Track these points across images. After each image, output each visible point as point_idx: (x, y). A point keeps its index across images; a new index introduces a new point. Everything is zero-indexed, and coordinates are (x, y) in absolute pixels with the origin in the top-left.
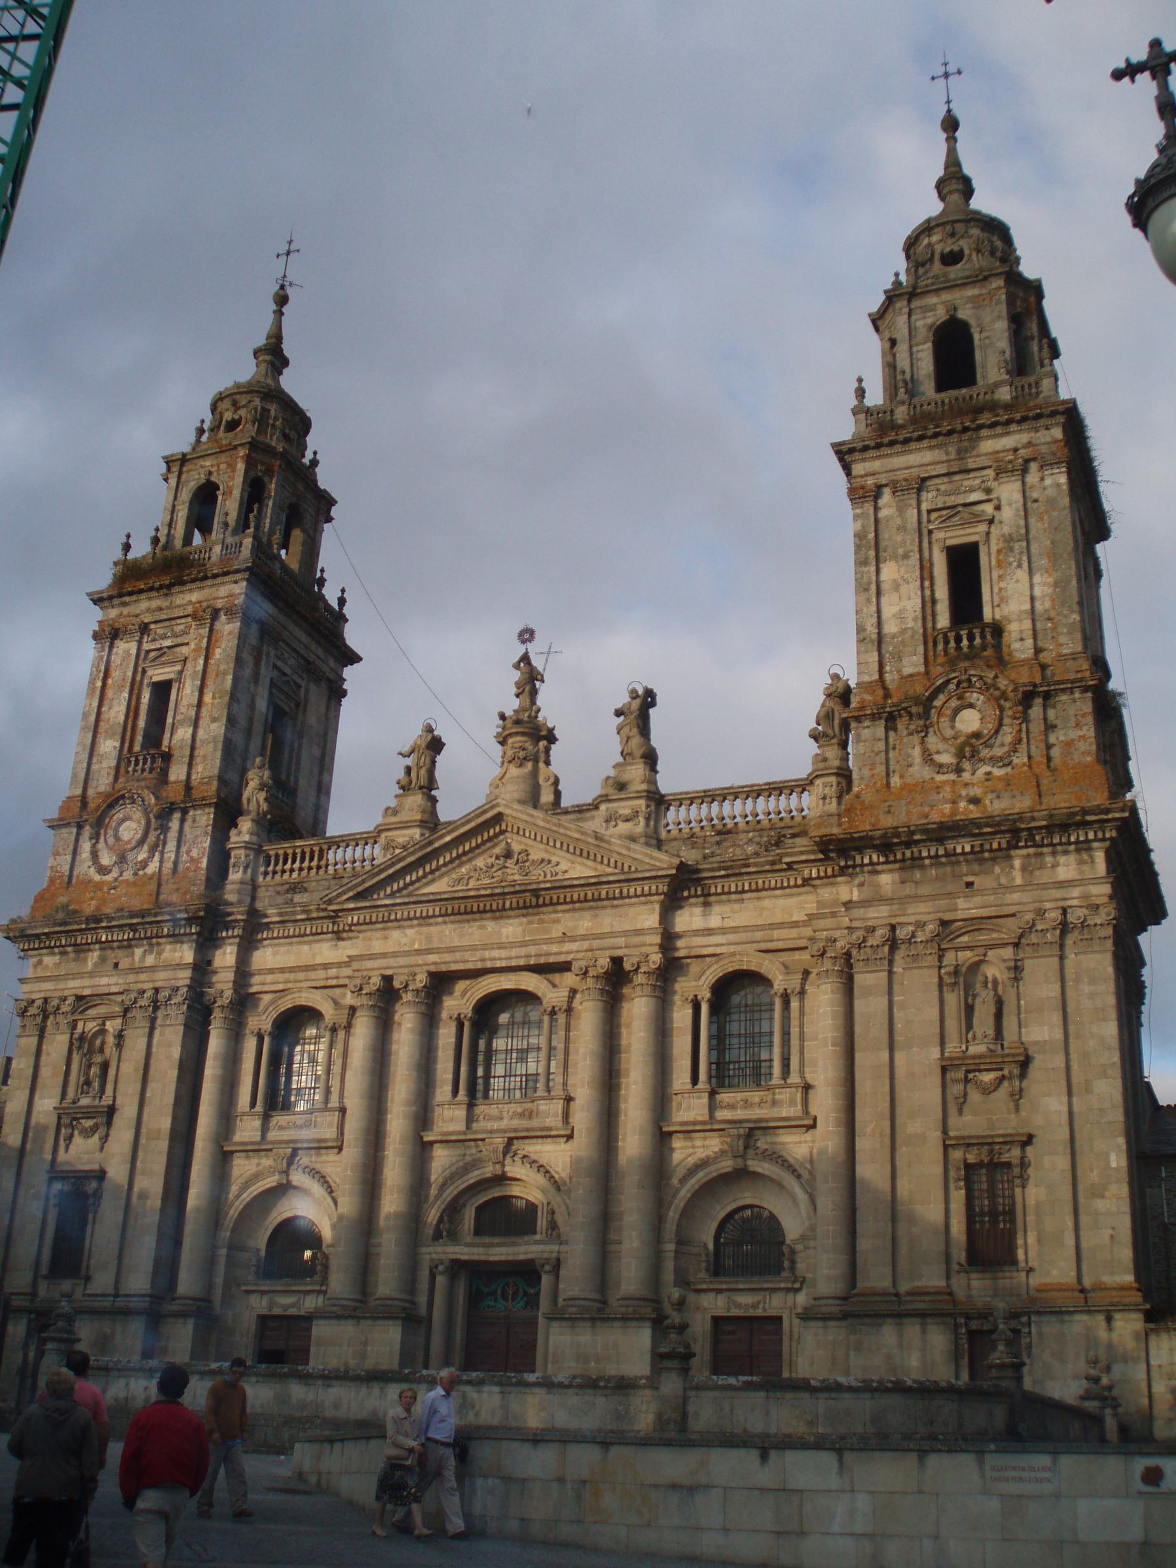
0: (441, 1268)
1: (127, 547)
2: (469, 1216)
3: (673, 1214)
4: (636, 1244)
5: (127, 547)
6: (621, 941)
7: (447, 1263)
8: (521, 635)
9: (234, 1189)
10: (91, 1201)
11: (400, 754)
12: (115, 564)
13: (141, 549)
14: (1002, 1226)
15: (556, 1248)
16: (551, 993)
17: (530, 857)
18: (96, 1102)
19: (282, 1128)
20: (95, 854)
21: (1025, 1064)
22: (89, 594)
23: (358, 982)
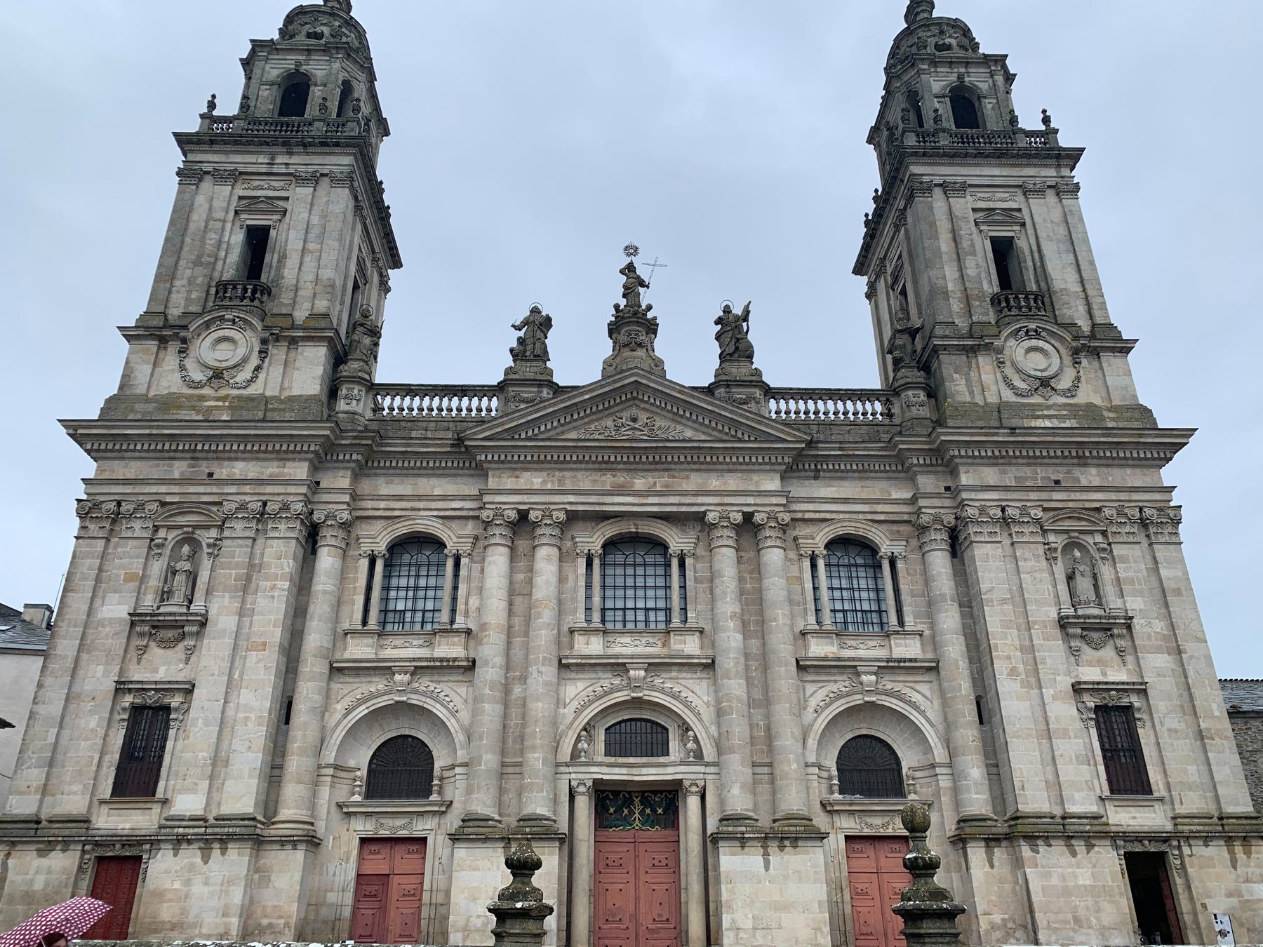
0: (582, 789)
1: (212, 105)
2: (601, 736)
3: (812, 742)
4: (794, 766)
5: (212, 105)
6: (751, 500)
7: (590, 783)
8: (626, 248)
9: (340, 707)
10: (172, 716)
11: (513, 326)
12: (202, 116)
13: (229, 106)
14: (1123, 760)
15: (702, 769)
16: (677, 540)
17: (657, 424)
18: (184, 610)
19: (396, 647)
20: (182, 368)
21: (1129, 627)
22: (175, 134)
23: (491, 513)
